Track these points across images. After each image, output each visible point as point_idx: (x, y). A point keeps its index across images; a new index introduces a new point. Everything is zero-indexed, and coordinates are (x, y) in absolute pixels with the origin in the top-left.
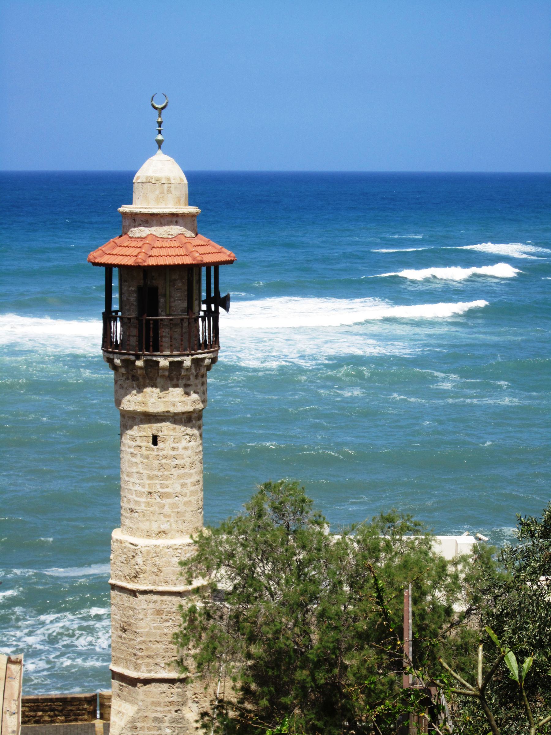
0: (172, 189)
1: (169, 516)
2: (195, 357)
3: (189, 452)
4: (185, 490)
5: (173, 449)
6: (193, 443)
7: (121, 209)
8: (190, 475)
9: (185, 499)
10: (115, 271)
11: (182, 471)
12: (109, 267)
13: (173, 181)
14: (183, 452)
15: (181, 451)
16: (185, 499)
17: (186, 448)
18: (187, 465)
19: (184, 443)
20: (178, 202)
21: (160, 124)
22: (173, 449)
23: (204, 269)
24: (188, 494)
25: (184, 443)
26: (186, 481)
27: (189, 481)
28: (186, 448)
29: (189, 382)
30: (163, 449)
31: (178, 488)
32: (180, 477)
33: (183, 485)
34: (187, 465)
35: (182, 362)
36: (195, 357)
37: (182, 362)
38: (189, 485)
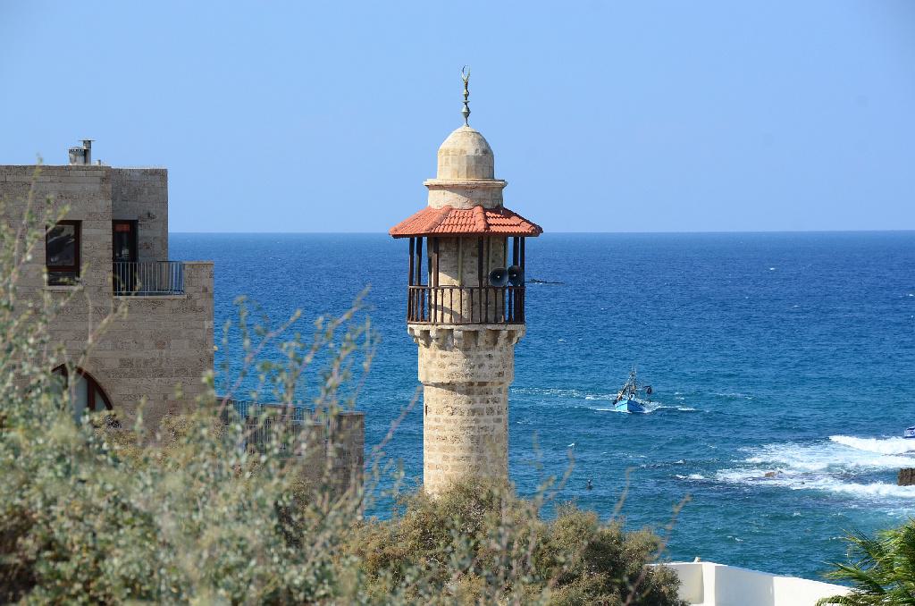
5: (436, 420)
6: (454, 417)
9: (447, 473)
11: (443, 443)
15: (442, 423)
17: (448, 421)
21: (466, 96)
23: (511, 239)
25: (446, 415)
26: (447, 454)
27: (451, 455)
28: (448, 421)
32: (443, 449)
33: (445, 458)
35: (428, 331)
37: (428, 331)
38: (451, 459)
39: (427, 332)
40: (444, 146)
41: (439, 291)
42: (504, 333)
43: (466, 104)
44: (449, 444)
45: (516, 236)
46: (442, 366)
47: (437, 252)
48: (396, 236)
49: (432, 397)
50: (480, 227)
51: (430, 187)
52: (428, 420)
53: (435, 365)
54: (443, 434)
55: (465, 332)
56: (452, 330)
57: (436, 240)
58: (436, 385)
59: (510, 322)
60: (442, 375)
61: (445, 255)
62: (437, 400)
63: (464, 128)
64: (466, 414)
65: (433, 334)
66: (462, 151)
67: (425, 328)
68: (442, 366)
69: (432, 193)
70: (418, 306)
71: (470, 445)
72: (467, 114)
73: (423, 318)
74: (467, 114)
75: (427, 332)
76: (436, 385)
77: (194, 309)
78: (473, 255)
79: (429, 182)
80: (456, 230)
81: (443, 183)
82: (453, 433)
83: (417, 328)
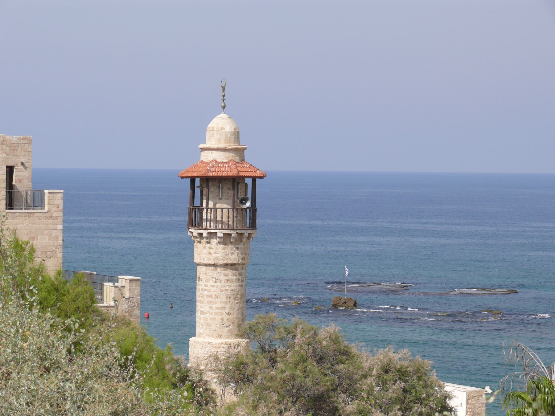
0: (215, 134)
1: (203, 325)
2: (209, 231)
3: (215, 289)
4: (211, 311)
5: (205, 285)
7: (199, 146)
8: (216, 303)
9: (212, 316)
10: (198, 181)
11: (209, 299)
12: (193, 180)
13: (215, 129)
14: (210, 288)
16: (212, 316)
17: (212, 286)
18: (213, 296)
19: (211, 283)
20: (219, 140)
21: (224, 96)
22: (205, 285)
23: (249, 181)
24: (214, 314)
25: (211, 283)
26: (212, 305)
27: (214, 306)
28: (212, 286)
29: (211, 246)
30: (201, 285)
31: (208, 309)
32: (209, 302)
33: (210, 308)
34: (213, 296)
36: (209, 231)
38: (214, 308)
39: (201, 234)
40: (211, 125)
41: (209, 210)
42: (247, 235)
43: (223, 101)
44: (214, 300)
45: (254, 179)
46: (210, 254)
47: (208, 187)
48: (182, 177)
49: (200, 270)
50: (234, 173)
51: (203, 149)
52: (200, 286)
53: (208, 252)
54: (210, 294)
55: (224, 234)
56: (216, 233)
57: (207, 180)
58: (206, 265)
59: (248, 229)
60: (209, 259)
61: (212, 189)
62: (206, 274)
63: (223, 115)
64: (223, 282)
65: (205, 235)
66: (222, 129)
67: (200, 231)
68: (210, 254)
69: (203, 153)
70: (195, 218)
71: (226, 300)
72: (224, 107)
73: (199, 225)
74: (224, 107)
75: (201, 234)
76: (206, 265)
77: (51, 218)
78: (229, 189)
79: (202, 146)
80: (220, 174)
81: (212, 147)
82: (215, 293)
83: (195, 232)
